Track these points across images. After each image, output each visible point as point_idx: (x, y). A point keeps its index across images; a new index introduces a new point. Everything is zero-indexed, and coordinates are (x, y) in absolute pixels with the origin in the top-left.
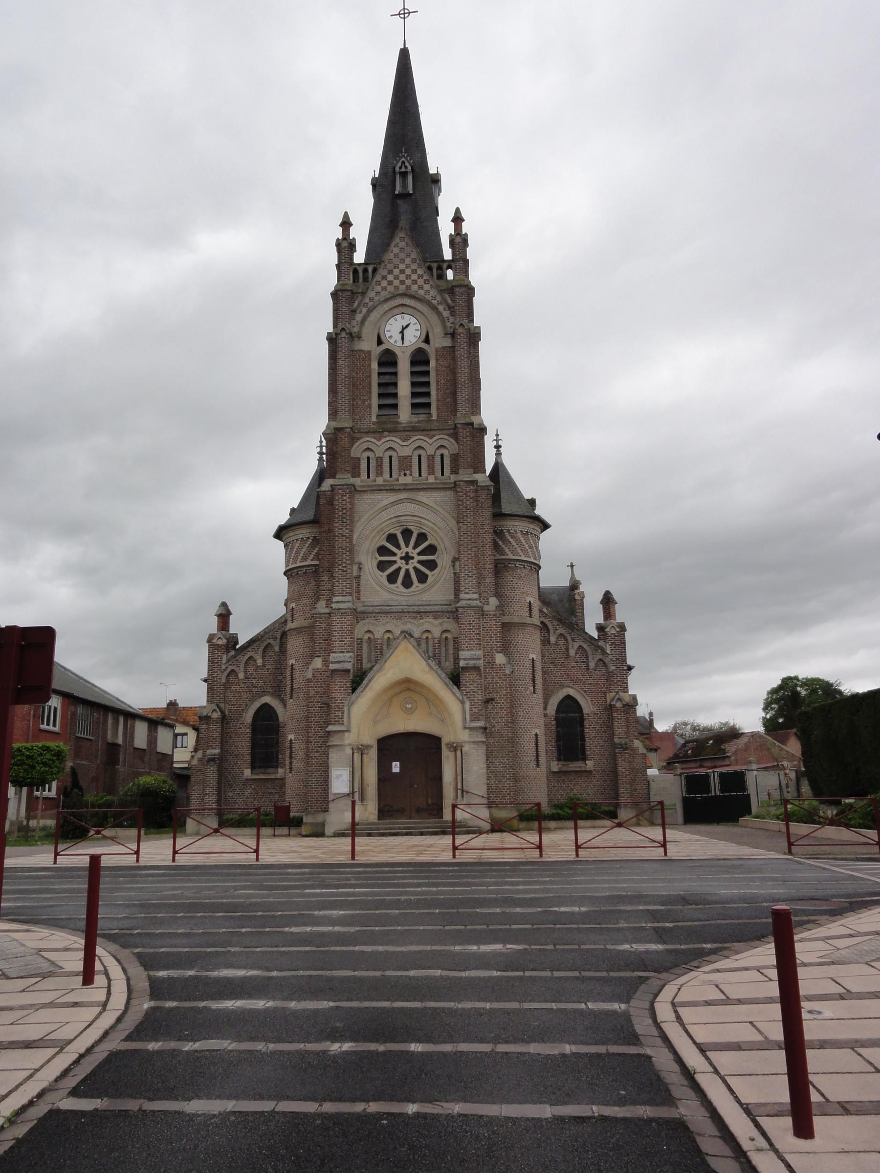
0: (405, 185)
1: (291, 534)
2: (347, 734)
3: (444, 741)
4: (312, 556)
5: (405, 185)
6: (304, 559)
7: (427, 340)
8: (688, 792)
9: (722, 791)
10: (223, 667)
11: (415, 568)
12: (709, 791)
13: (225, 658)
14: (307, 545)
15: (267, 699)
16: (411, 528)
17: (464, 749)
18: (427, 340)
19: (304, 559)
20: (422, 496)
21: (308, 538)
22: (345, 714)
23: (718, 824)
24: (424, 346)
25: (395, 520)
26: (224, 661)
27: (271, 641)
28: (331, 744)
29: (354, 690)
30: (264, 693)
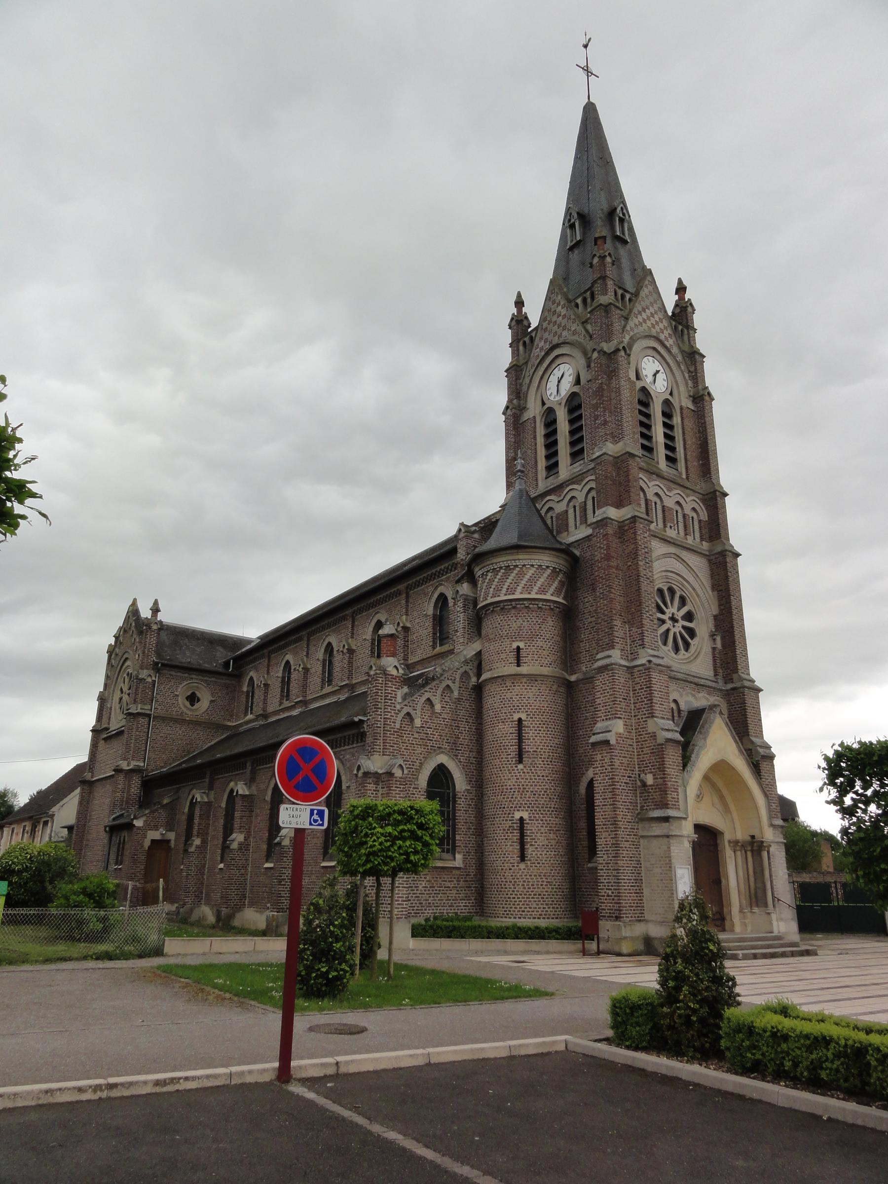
0: (597, 228)
1: (521, 557)
2: (683, 822)
3: (727, 837)
4: (504, 590)
5: (597, 228)
6: (542, 591)
7: (671, 394)
8: (803, 899)
9: (846, 900)
10: (398, 707)
11: (675, 634)
12: (831, 901)
13: (400, 694)
14: (545, 575)
15: (443, 759)
16: (675, 587)
17: (772, 849)
18: (671, 394)
19: (542, 591)
20: (685, 555)
21: (548, 567)
22: (681, 797)
23: (842, 934)
24: (670, 398)
25: (664, 574)
26: (399, 699)
27: (450, 683)
28: (674, 833)
29: (685, 766)
30: (439, 750)
